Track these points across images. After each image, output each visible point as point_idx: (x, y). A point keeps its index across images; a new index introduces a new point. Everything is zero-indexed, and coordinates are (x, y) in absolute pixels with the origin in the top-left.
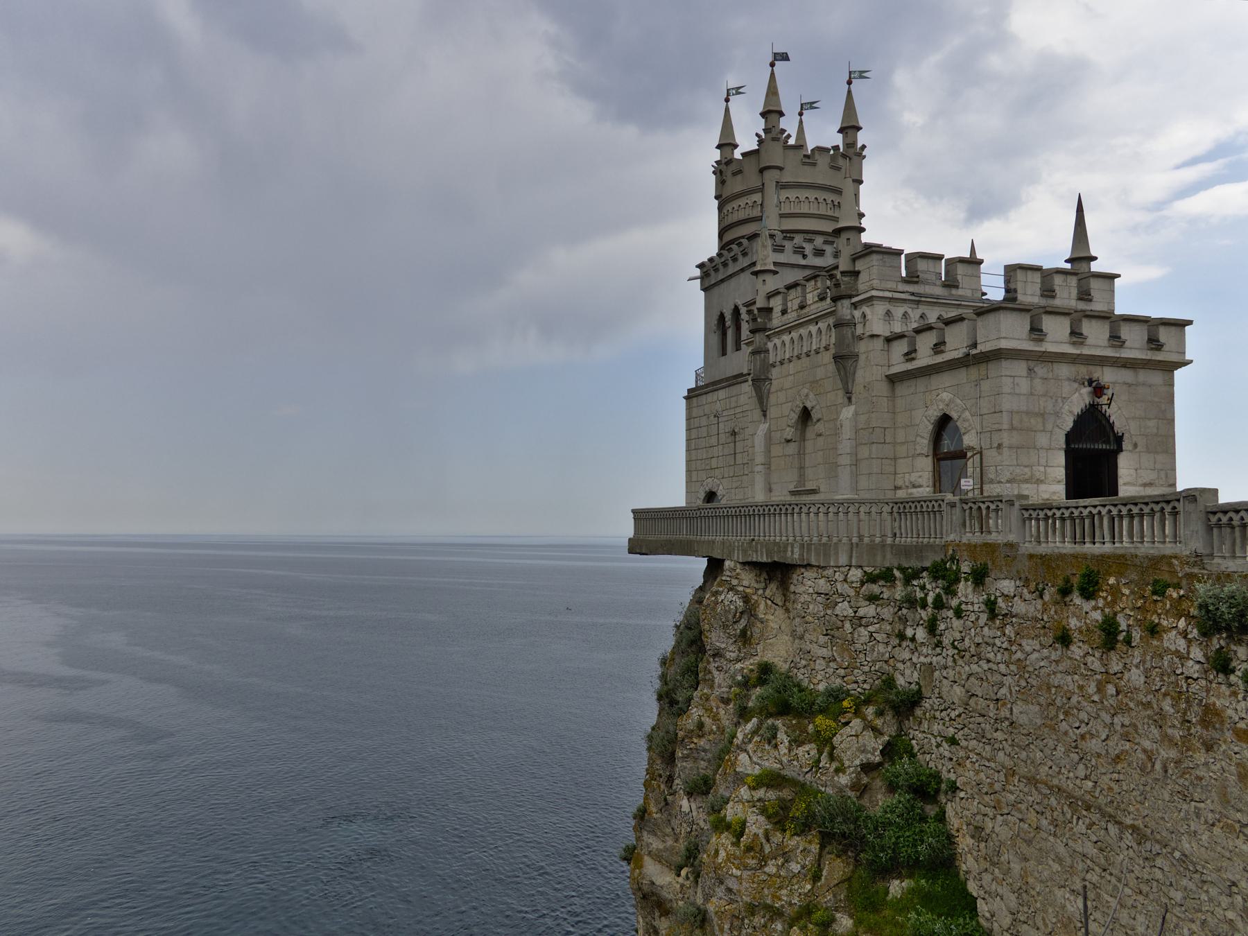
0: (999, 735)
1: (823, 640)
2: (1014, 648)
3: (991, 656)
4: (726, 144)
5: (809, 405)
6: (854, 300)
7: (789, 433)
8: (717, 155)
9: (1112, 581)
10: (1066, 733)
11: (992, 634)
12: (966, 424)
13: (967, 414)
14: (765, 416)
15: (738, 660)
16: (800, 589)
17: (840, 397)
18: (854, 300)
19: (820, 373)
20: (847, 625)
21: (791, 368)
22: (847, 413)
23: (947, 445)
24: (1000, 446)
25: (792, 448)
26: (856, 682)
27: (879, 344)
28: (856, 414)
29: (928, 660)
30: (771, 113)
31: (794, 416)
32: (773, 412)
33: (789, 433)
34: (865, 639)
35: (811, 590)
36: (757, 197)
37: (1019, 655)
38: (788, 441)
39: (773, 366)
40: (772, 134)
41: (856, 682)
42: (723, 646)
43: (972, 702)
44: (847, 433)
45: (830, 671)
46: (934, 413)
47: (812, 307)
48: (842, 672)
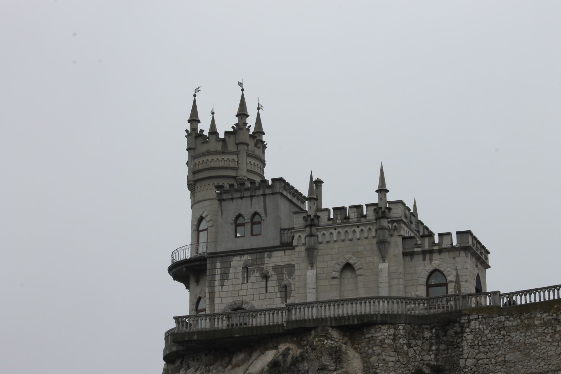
0: (498, 367)
1: (393, 354)
2: (506, 337)
3: (493, 343)
4: (194, 120)
5: (351, 262)
6: (389, 220)
7: (336, 274)
8: (188, 126)
9: (555, 306)
10: (535, 355)
11: (493, 335)
12: (449, 273)
13: (449, 269)
14: (312, 267)
15: (335, 370)
16: (379, 334)
17: (376, 259)
18: (389, 220)
19: (360, 249)
20: (405, 347)
21: (336, 245)
22: (384, 266)
23: (433, 281)
24: (466, 281)
25: (336, 282)
26: (409, 370)
27: (400, 240)
28: (389, 266)
29: (449, 355)
30: (242, 114)
31: (339, 268)
32: (319, 264)
33: (336, 274)
34: (412, 352)
35: (386, 334)
36: (235, 157)
37: (509, 338)
38: (334, 278)
39: (320, 243)
40: (241, 127)
41: (409, 370)
42: (328, 364)
43: (480, 362)
44: (385, 274)
45: (397, 366)
46: (430, 268)
47: (354, 220)
48: (403, 366)
